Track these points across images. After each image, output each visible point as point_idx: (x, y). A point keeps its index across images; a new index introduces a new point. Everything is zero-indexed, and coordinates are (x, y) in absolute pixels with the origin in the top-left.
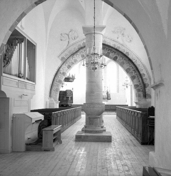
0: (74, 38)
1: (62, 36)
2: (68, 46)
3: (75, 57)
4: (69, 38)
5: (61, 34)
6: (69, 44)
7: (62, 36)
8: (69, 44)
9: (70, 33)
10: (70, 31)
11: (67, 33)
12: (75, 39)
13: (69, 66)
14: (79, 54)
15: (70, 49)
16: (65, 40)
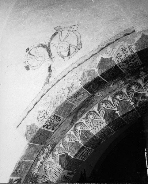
0: (66, 54)
1: (29, 53)
2: (47, 82)
3: (83, 121)
4: (50, 56)
5: (28, 50)
6: (50, 74)
7: (29, 53)
8: (50, 74)
9: (55, 41)
10: (55, 34)
11: (46, 43)
12: (69, 54)
13: (63, 156)
14: (95, 109)
15: (53, 93)
16: (38, 67)
